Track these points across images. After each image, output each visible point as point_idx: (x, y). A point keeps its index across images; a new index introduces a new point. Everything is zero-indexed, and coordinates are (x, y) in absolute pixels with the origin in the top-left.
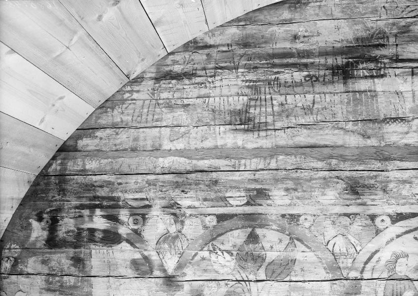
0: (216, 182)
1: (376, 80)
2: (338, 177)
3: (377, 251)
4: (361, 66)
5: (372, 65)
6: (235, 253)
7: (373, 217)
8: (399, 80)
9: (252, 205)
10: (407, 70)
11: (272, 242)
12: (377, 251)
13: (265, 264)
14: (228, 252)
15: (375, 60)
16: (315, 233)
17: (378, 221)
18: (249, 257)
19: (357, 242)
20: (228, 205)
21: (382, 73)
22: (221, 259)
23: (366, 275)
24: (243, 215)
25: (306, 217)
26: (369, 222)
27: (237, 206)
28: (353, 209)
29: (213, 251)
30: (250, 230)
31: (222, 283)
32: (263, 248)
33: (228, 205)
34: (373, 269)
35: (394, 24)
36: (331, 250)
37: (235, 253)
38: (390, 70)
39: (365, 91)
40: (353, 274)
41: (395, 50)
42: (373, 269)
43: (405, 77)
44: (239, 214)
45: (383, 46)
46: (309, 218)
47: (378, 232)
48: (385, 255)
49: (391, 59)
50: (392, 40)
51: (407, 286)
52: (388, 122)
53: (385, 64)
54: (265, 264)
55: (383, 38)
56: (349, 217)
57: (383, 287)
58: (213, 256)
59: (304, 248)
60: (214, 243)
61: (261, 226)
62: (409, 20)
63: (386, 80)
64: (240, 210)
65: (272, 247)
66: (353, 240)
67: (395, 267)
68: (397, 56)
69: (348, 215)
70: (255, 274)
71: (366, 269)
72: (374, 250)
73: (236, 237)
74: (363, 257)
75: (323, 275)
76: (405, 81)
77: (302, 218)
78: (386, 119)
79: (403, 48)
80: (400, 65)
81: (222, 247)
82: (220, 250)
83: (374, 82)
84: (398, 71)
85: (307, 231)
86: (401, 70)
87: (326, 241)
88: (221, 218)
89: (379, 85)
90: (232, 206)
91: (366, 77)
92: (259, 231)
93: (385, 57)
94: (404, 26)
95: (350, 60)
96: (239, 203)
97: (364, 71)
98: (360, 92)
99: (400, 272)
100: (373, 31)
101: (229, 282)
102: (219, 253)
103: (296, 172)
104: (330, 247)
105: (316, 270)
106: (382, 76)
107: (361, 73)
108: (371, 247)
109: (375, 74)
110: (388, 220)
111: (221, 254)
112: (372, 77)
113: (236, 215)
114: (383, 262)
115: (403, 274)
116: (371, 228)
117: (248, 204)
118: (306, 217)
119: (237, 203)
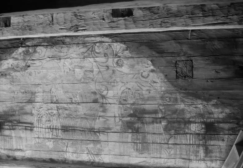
1: (12, 130)
4: (6, 124)
5: (10, 124)
8: (21, 132)
10: (23, 127)
15: (11, 121)
21: (14, 128)
35: (17, 106)
38: (17, 127)
39: (8, 136)
41: (18, 118)
43: (23, 130)
45: (14, 115)
49: (17, 122)
50: (17, 113)
52: (16, 151)
53: (15, 123)
55: (14, 112)
62: (23, 104)
63: (16, 131)
68: (19, 120)
76: (23, 132)
78: (16, 149)
79: (22, 117)
80: (21, 125)
83: (11, 132)
84: (20, 128)
86: (21, 127)
89: (13, 133)
91: (8, 129)
93: (15, 120)
94: (21, 107)
95: (2, 121)
97: (7, 126)
98: (6, 136)
100: (10, 108)
106: (14, 129)
107: (6, 127)
109: (11, 128)
112: (10, 129)
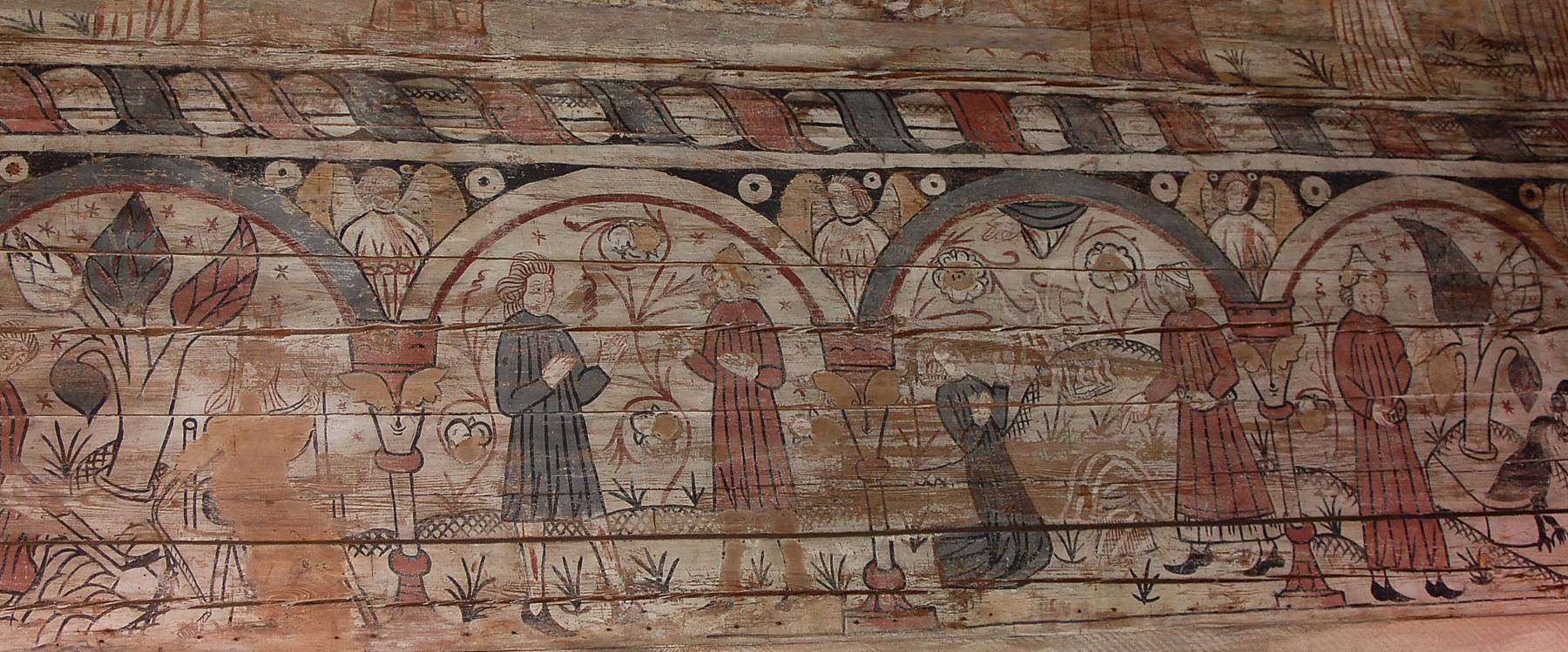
0: (37, 70)
2: (368, 72)
3: (470, 257)
6: (83, 258)
7: (459, 171)
9: (133, 132)
11: (191, 224)
12: (470, 257)
13: (171, 287)
14: (67, 255)
16: (310, 207)
17: (473, 179)
18: (122, 269)
19: (420, 231)
20: (66, 129)
22: (41, 273)
23: (449, 317)
24: (108, 156)
25: (283, 166)
26: (448, 182)
27: (90, 132)
28: (408, 150)
29: (24, 249)
30: (128, 195)
31: (44, 338)
32: (162, 240)
33: (66, 129)
34: (465, 301)
36: (352, 251)
37: (83, 258)
40: (413, 313)
42: (465, 301)
44: (97, 155)
46: (292, 168)
47: (473, 206)
48: (495, 271)
51: (555, 346)
54: (171, 287)
56: (397, 169)
57: (492, 345)
58: (20, 267)
59: (277, 244)
60: (24, 226)
61: (158, 186)
64: (99, 144)
65: (188, 241)
66: (409, 227)
67: (521, 297)
69: (395, 165)
70: (142, 313)
71: (447, 300)
72: (463, 252)
73: (83, 217)
74: (436, 272)
75: (331, 315)
77: (273, 168)
81: (44, 239)
82: (40, 246)
85: (285, 201)
87: (338, 226)
88: (43, 163)
90: (73, 131)
92: (149, 199)
96: (94, 124)
99: (536, 308)
101: (65, 337)
102: (38, 256)
103: (255, 52)
104: (349, 241)
105: (311, 302)
108: (459, 243)
110: (497, 181)
111: (44, 260)
113: (88, 157)
114: (489, 284)
115: (542, 312)
116: (455, 197)
117: (121, 128)
118: (283, 166)
119: (90, 124)
